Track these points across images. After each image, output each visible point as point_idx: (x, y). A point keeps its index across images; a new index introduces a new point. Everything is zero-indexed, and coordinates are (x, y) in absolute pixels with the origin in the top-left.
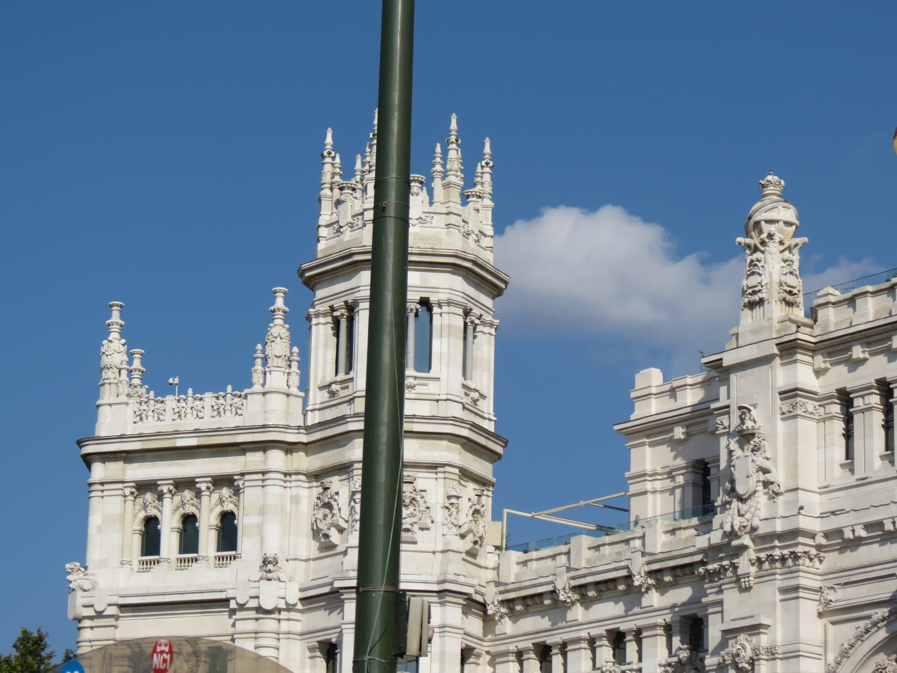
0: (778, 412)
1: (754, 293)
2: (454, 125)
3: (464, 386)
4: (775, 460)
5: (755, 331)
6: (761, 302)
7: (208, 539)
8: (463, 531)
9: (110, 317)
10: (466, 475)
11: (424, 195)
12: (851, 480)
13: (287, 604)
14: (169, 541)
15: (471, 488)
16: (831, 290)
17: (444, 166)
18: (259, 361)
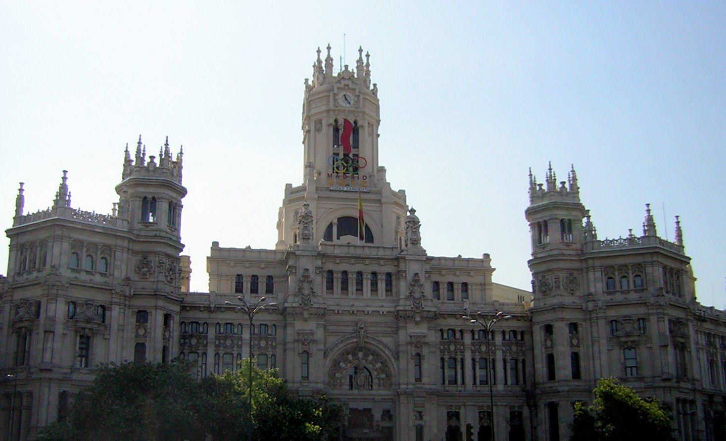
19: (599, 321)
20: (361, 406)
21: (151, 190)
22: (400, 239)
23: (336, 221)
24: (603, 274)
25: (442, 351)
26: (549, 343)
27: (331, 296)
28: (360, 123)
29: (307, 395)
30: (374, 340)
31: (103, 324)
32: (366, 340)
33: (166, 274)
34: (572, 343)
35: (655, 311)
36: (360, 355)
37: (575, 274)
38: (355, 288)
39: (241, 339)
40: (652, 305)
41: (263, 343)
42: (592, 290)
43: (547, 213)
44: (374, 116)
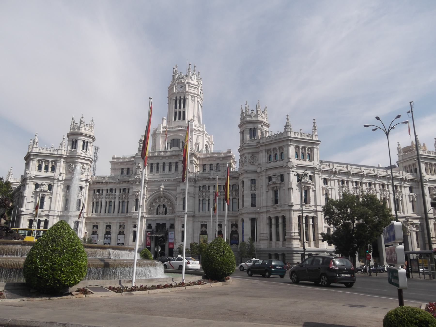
12: (152, 174)
19: (263, 177)
20: (161, 222)
21: (75, 137)
22: (198, 147)
23: (170, 141)
24: (267, 153)
25: (199, 196)
26: (243, 189)
27: (152, 174)
28: (186, 97)
30: (167, 192)
32: (164, 193)
34: (251, 189)
35: (287, 170)
36: (162, 199)
37: (256, 155)
38: (162, 170)
39: (115, 195)
40: (286, 167)
41: (124, 196)
42: (261, 162)
43: (244, 126)
44: (197, 93)
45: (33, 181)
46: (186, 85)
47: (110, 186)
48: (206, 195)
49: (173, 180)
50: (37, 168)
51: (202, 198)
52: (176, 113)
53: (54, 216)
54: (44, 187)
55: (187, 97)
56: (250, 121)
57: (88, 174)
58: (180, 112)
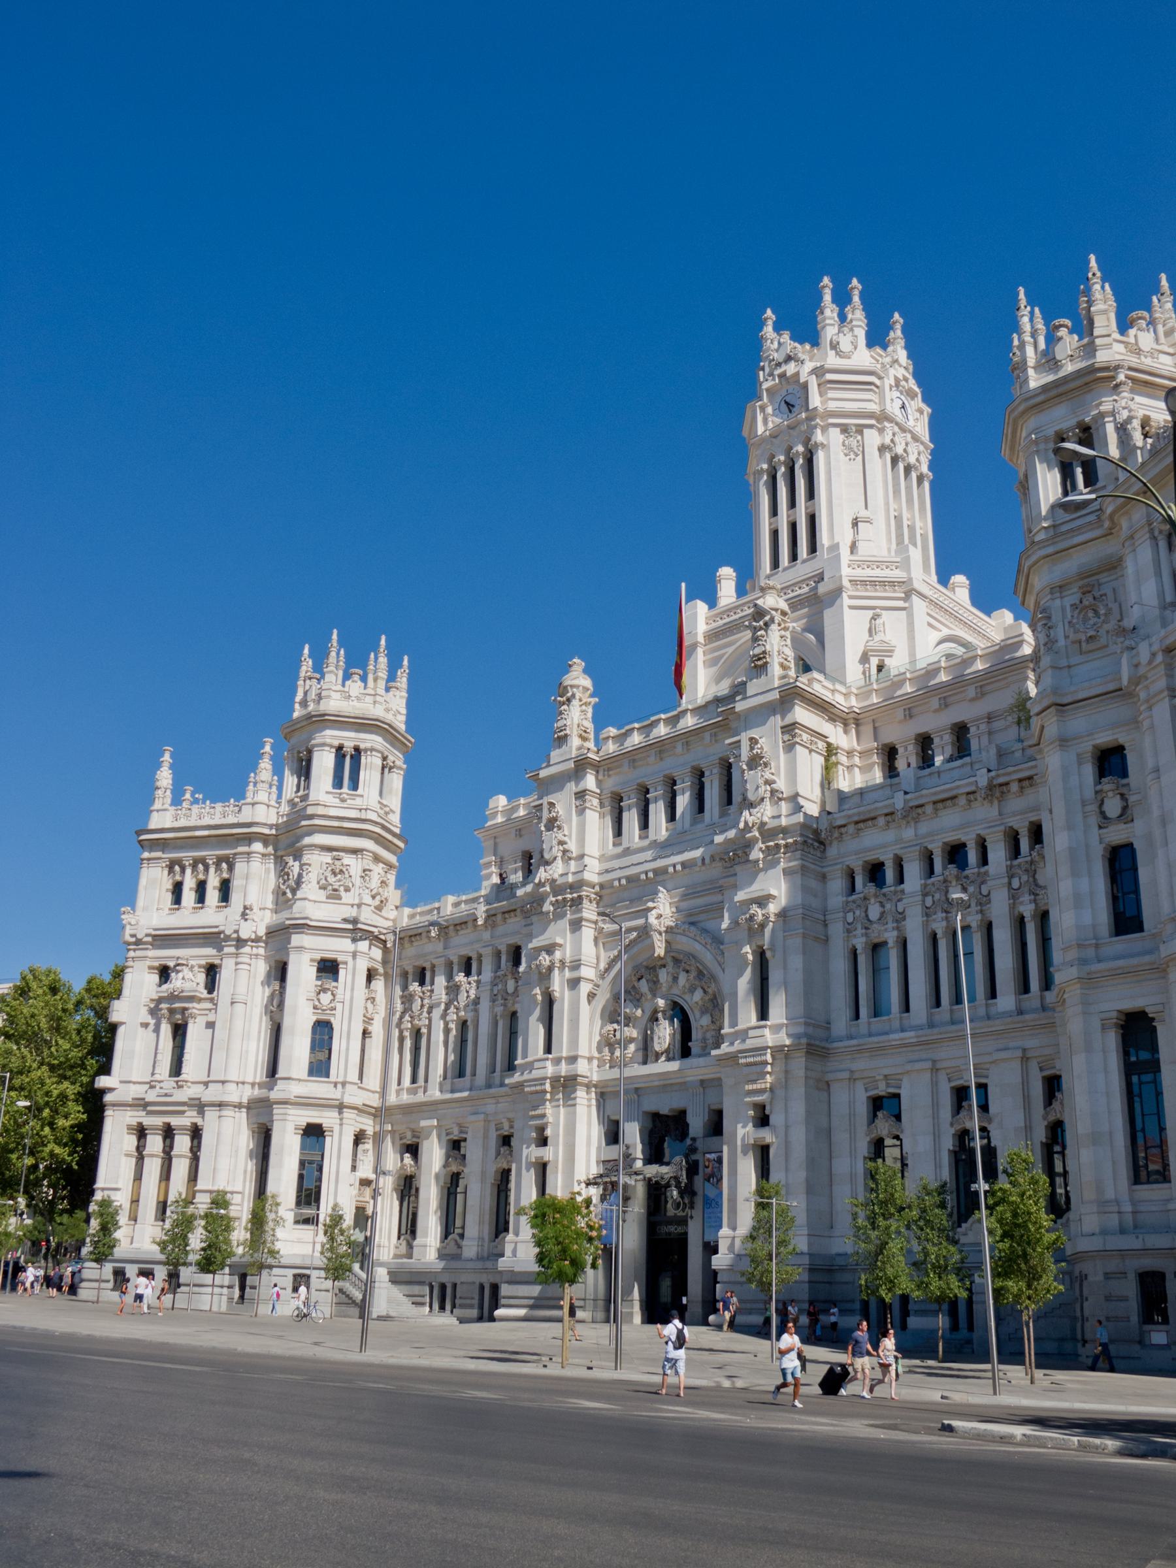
0: (574, 806)
1: (562, 731)
2: (383, 642)
3: (379, 802)
4: (570, 837)
5: (562, 755)
6: (566, 735)
7: (212, 895)
8: (373, 893)
9: (163, 756)
10: (377, 859)
11: (360, 684)
12: (619, 850)
13: (256, 935)
14: (189, 896)
15: (379, 869)
16: (611, 729)
17: (375, 666)
18: (251, 784)
29: (538, 1088)
31: (210, 996)
33: (323, 881)
34: (1103, 814)
36: (663, 976)
45: (152, 953)
46: (806, 383)
47: (462, 945)
48: (882, 914)
49: (707, 861)
50: (169, 897)
51: (864, 939)
52: (775, 534)
53: (221, 1105)
54: (183, 979)
55: (819, 437)
56: (1045, 388)
57: (361, 899)
58: (793, 527)
